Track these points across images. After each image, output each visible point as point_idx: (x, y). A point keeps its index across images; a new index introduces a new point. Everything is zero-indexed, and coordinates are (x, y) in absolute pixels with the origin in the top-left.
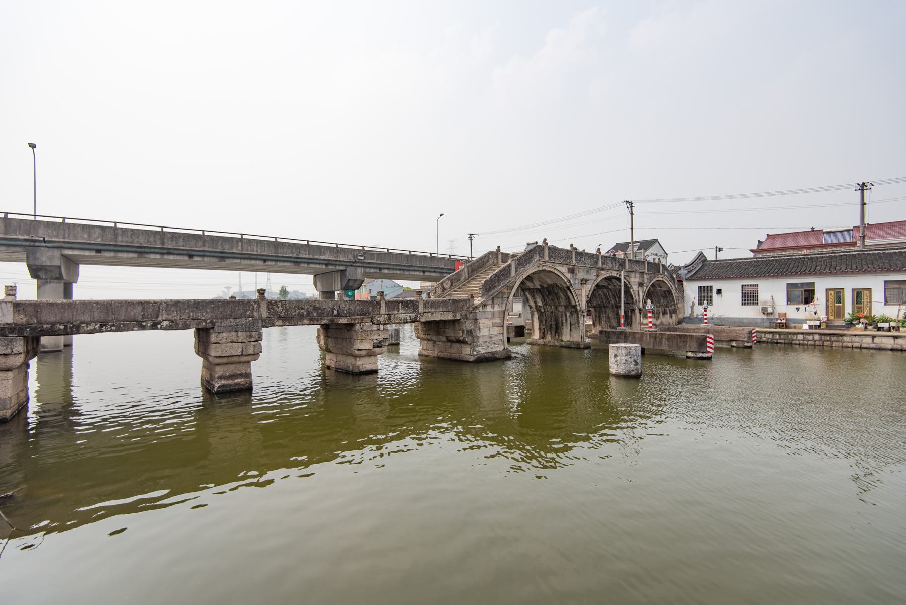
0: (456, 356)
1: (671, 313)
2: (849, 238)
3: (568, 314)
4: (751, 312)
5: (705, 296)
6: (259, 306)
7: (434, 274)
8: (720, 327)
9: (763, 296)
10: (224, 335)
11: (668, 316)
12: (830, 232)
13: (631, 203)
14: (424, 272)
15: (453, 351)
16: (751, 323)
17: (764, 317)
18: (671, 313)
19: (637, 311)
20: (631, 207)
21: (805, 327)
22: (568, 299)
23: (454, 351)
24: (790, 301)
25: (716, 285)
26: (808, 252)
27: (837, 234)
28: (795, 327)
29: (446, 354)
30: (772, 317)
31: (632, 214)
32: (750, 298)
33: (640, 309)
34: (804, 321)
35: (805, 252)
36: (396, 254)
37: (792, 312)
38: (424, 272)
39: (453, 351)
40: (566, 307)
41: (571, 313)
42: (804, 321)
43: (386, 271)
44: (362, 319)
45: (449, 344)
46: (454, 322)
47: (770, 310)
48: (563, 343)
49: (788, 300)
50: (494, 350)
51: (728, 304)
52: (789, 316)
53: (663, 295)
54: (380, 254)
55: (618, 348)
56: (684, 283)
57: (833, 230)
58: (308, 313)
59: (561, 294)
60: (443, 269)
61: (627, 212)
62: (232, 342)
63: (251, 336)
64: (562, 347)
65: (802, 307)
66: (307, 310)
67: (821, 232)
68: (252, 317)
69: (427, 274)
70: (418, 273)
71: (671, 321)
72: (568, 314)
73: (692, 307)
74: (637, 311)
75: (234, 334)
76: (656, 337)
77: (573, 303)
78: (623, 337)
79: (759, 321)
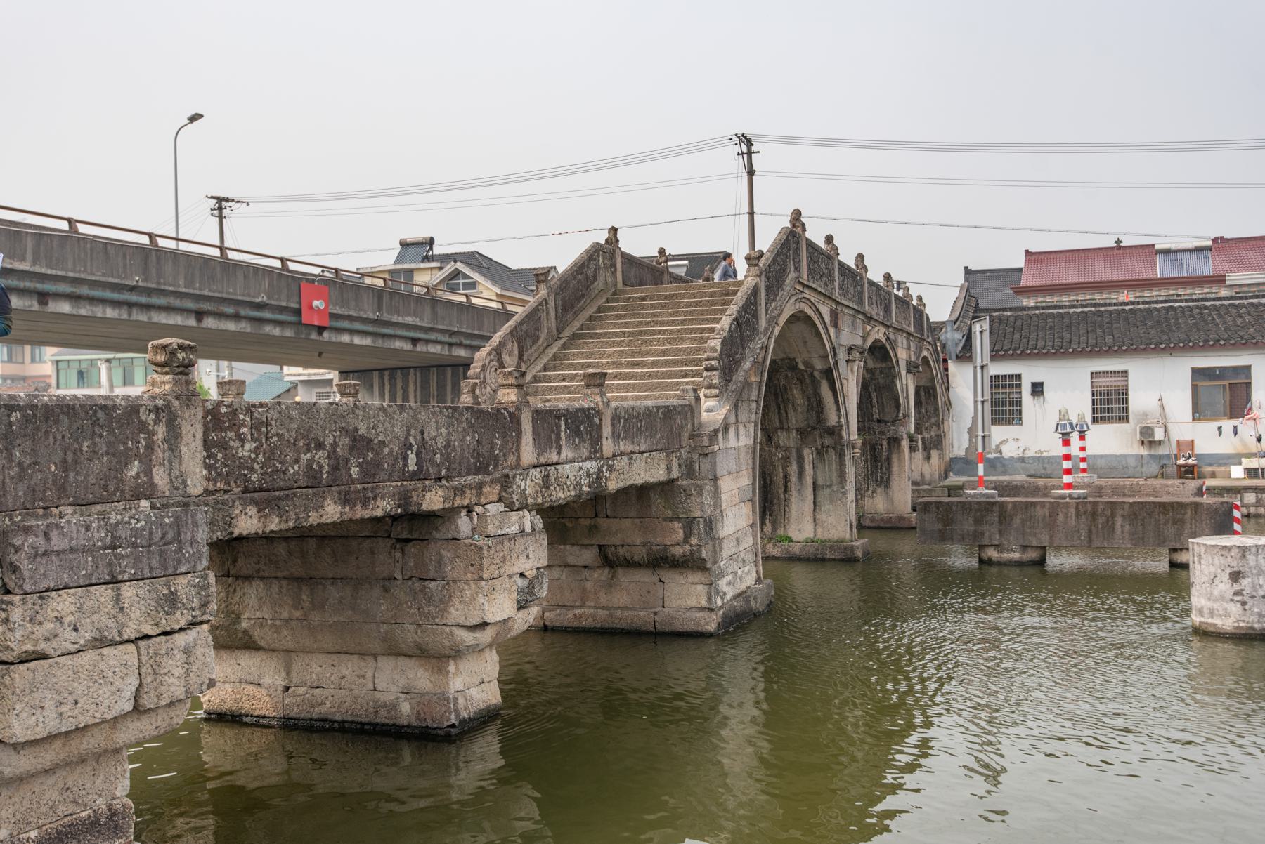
0: (642, 618)
1: (927, 449)
2: (1207, 267)
3: (808, 455)
4: (1109, 441)
5: (1004, 407)
6: (174, 435)
7: (231, 326)
8: (1041, 482)
9: (1141, 399)
10: (64, 603)
11: (919, 455)
12: (1168, 251)
13: (749, 143)
14: (200, 315)
15: (620, 598)
16: (1113, 466)
17: (1144, 451)
18: (927, 449)
19: (905, 443)
20: (750, 153)
21: (1237, 472)
22: (817, 407)
23: (626, 598)
24: (1199, 412)
25: (1030, 372)
26: (1131, 298)
27: (1185, 256)
28: (1213, 475)
29: (587, 614)
30: (1162, 451)
31: (751, 172)
32: (1110, 404)
33: (911, 439)
34: (1236, 458)
35: (1124, 296)
36: (106, 244)
37: (1210, 439)
38: (200, 315)
39: (620, 598)
40: (803, 433)
41: (820, 453)
42: (1236, 458)
43: (65, 307)
44: (480, 487)
45: (604, 574)
46: (667, 487)
47: (1159, 435)
48: (796, 549)
49: (1196, 408)
50: (743, 587)
51: (1052, 423)
52: (1202, 448)
53: (899, 400)
54: (43, 237)
55: (1244, 550)
56: (951, 365)
57: (1173, 247)
58: (338, 465)
59: (796, 394)
60: (260, 306)
61: (739, 165)
62: (100, 642)
63: (171, 602)
64: (792, 559)
65: (1228, 425)
66: (333, 455)
67: (1148, 251)
68: (148, 491)
69: (210, 323)
70: (177, 320)
71: (926, 470)
72: (808, 455)
73: (972, 431)
74: (905, 443)
75: (103, 594)
76: (1094, 515)
77: (832, 420)
78: (994, 517)
79: (1132, 462)
